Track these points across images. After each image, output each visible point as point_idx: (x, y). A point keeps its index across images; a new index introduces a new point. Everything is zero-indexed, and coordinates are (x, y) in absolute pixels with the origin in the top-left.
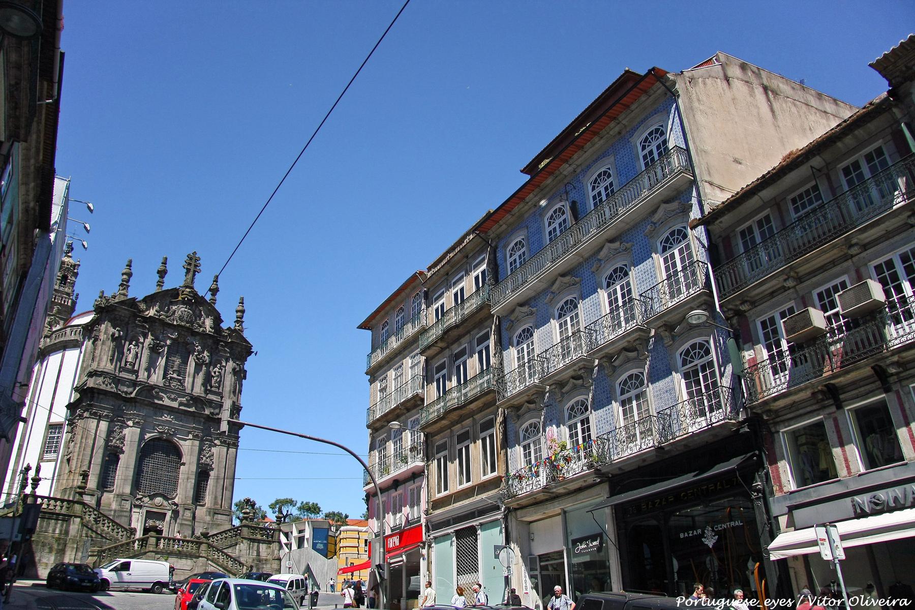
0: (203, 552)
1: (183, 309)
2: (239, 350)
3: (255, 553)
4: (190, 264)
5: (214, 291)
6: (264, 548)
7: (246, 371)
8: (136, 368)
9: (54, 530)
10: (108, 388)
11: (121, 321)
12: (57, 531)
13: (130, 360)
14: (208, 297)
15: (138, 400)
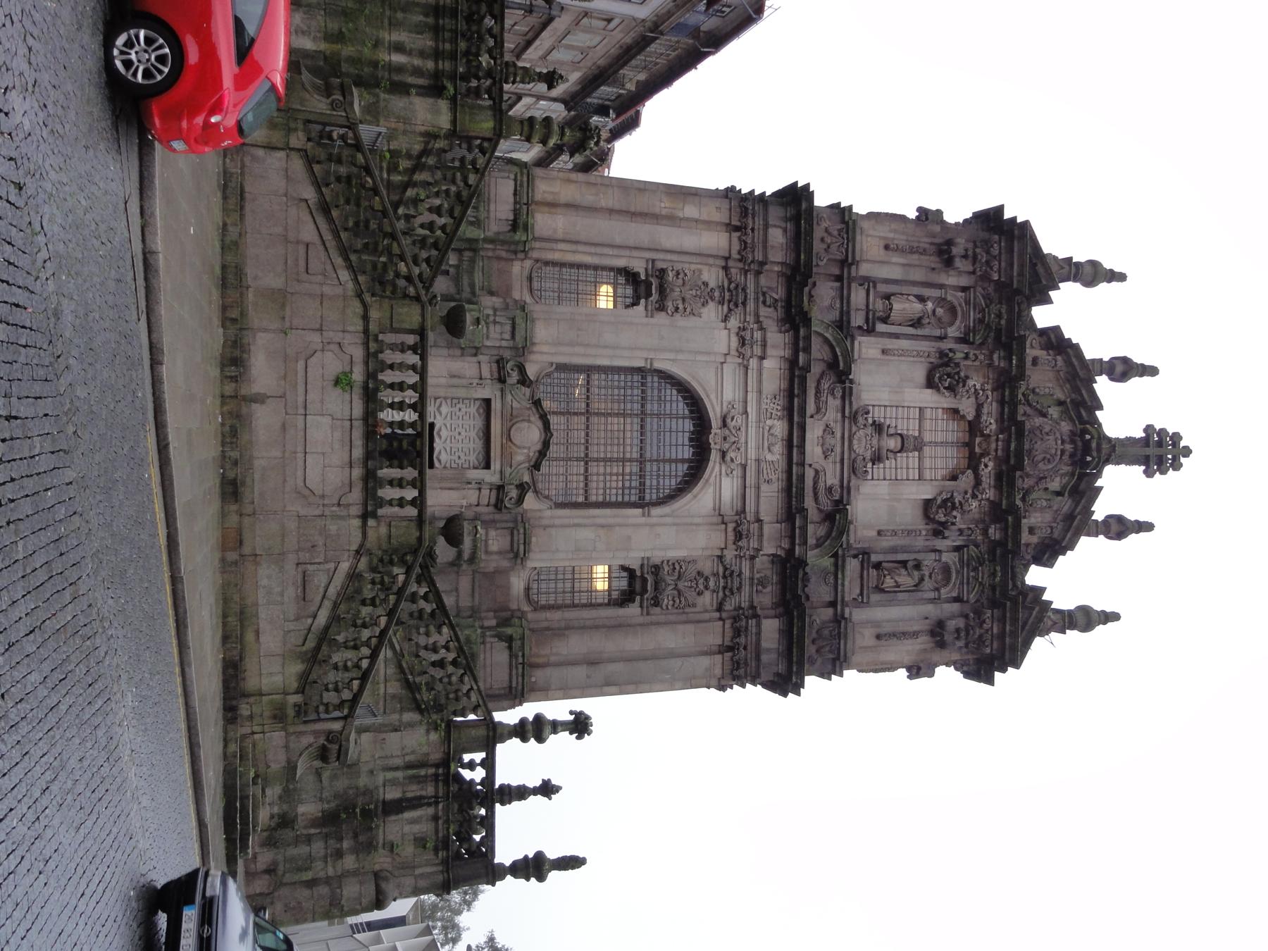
0: (383, 530)
1: (1058, 435)
2: (995, 630)
3: (393, 794)
4: (1160, 444)
5: (1119, 528)
6: (416, 828)
7: (931, 674)
8: (881, 327)
9: (399, 48)
10: (818, 246)
11: (987, 262)
12: (397, 58)
13: (897, 306)
14: (1100, 510)
15: (802, 332)
